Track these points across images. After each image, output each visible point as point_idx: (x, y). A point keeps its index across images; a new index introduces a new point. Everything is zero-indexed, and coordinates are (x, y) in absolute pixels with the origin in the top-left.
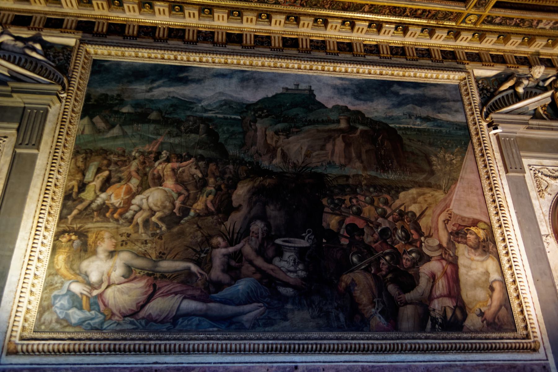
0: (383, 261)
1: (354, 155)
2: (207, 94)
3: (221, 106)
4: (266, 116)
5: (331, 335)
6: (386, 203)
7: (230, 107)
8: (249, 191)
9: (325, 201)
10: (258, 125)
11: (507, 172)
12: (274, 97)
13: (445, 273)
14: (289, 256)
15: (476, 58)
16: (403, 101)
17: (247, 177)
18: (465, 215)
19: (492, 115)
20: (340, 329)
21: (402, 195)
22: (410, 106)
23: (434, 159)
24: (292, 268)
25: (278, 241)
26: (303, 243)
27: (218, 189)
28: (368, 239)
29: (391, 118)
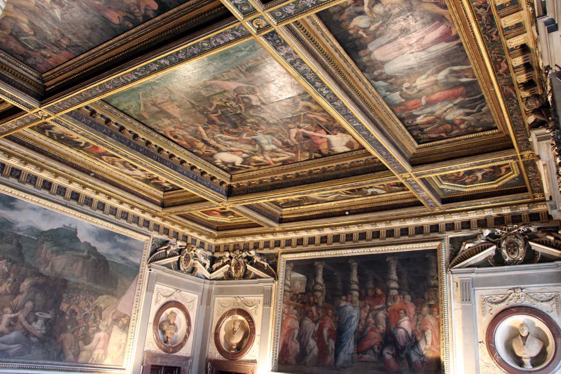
0: (81, 329)
1: (85, 272)
2: (23, 220)
3: (28, 229)
4: (50, 241)
5: (48, 362)
6: (91, 301)
7: (33, 231)
8: (30, 284)
9: (64, 295)
10: (44, 246)
11: (147, 291)
12: (57, 229)
13: (105, 338)
14: (40, 322)
15: (157, 228)
16: (117, 246)
17: (31, 276)
18: (123, 312)
19: (152, 264)
20: (53, 360)
21: (100, 297)
22: (119, 249)
23: (120, 281)
24: (40, 328)
25: (37, 314)
26: (48, 316)
27: (15, 280)
28: (78, 318)
29: (108, 255)
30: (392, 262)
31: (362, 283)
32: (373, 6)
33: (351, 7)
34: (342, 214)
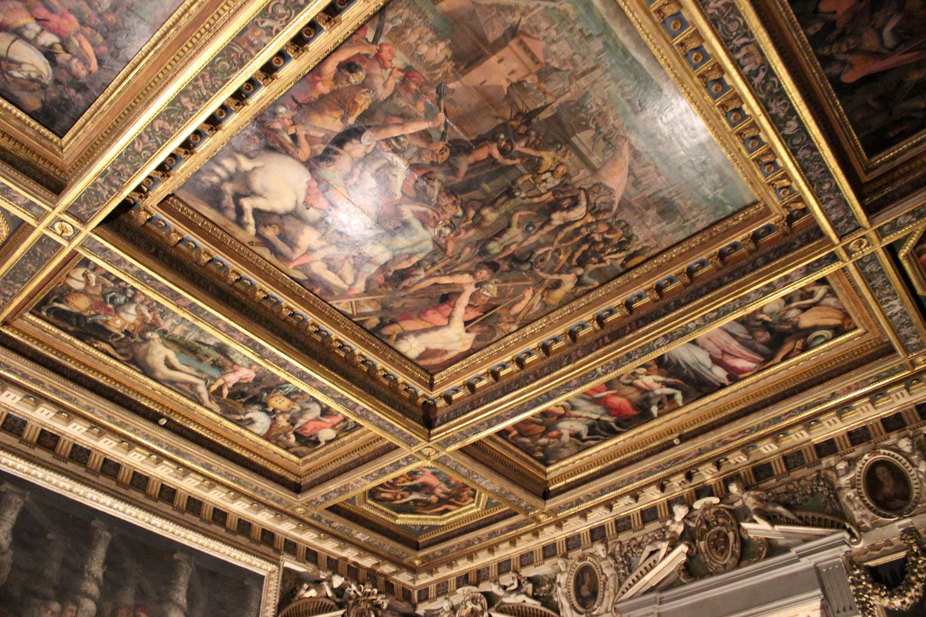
30: (184, 565)
31: (111, 585)
34: (152, 417)
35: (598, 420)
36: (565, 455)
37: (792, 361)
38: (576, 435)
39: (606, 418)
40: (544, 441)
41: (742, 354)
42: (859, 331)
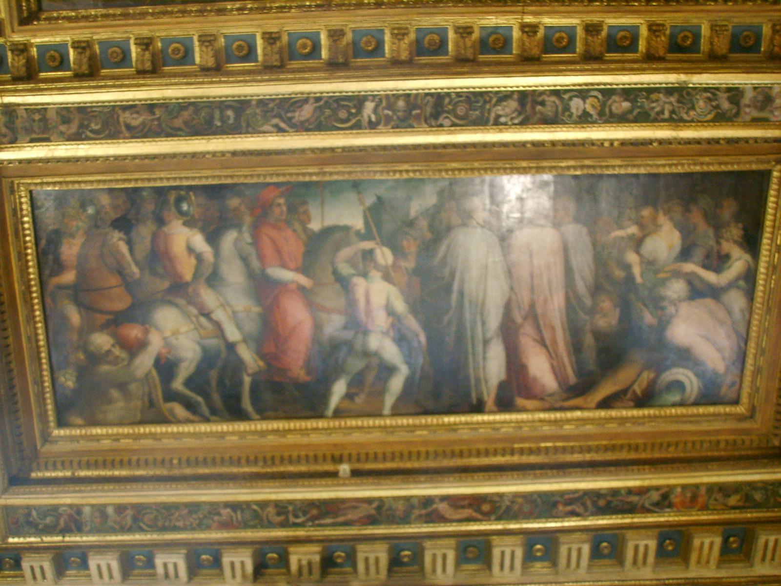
32: (690, 283)
33: (712, 243)
35: (231, 347)
36: (110, 416)
37: (613, 413)
38: (166, 367)
39: (246, 354)
40: (102, 341)
41: (554, 342)
42: (740, 409)
